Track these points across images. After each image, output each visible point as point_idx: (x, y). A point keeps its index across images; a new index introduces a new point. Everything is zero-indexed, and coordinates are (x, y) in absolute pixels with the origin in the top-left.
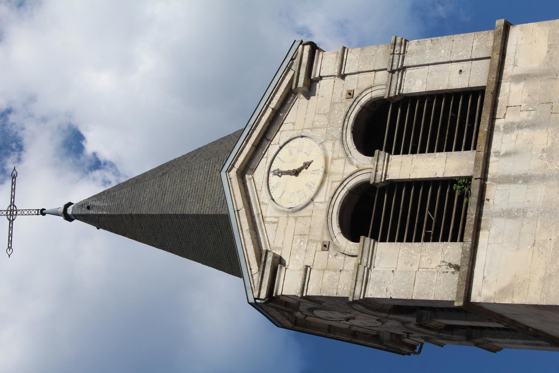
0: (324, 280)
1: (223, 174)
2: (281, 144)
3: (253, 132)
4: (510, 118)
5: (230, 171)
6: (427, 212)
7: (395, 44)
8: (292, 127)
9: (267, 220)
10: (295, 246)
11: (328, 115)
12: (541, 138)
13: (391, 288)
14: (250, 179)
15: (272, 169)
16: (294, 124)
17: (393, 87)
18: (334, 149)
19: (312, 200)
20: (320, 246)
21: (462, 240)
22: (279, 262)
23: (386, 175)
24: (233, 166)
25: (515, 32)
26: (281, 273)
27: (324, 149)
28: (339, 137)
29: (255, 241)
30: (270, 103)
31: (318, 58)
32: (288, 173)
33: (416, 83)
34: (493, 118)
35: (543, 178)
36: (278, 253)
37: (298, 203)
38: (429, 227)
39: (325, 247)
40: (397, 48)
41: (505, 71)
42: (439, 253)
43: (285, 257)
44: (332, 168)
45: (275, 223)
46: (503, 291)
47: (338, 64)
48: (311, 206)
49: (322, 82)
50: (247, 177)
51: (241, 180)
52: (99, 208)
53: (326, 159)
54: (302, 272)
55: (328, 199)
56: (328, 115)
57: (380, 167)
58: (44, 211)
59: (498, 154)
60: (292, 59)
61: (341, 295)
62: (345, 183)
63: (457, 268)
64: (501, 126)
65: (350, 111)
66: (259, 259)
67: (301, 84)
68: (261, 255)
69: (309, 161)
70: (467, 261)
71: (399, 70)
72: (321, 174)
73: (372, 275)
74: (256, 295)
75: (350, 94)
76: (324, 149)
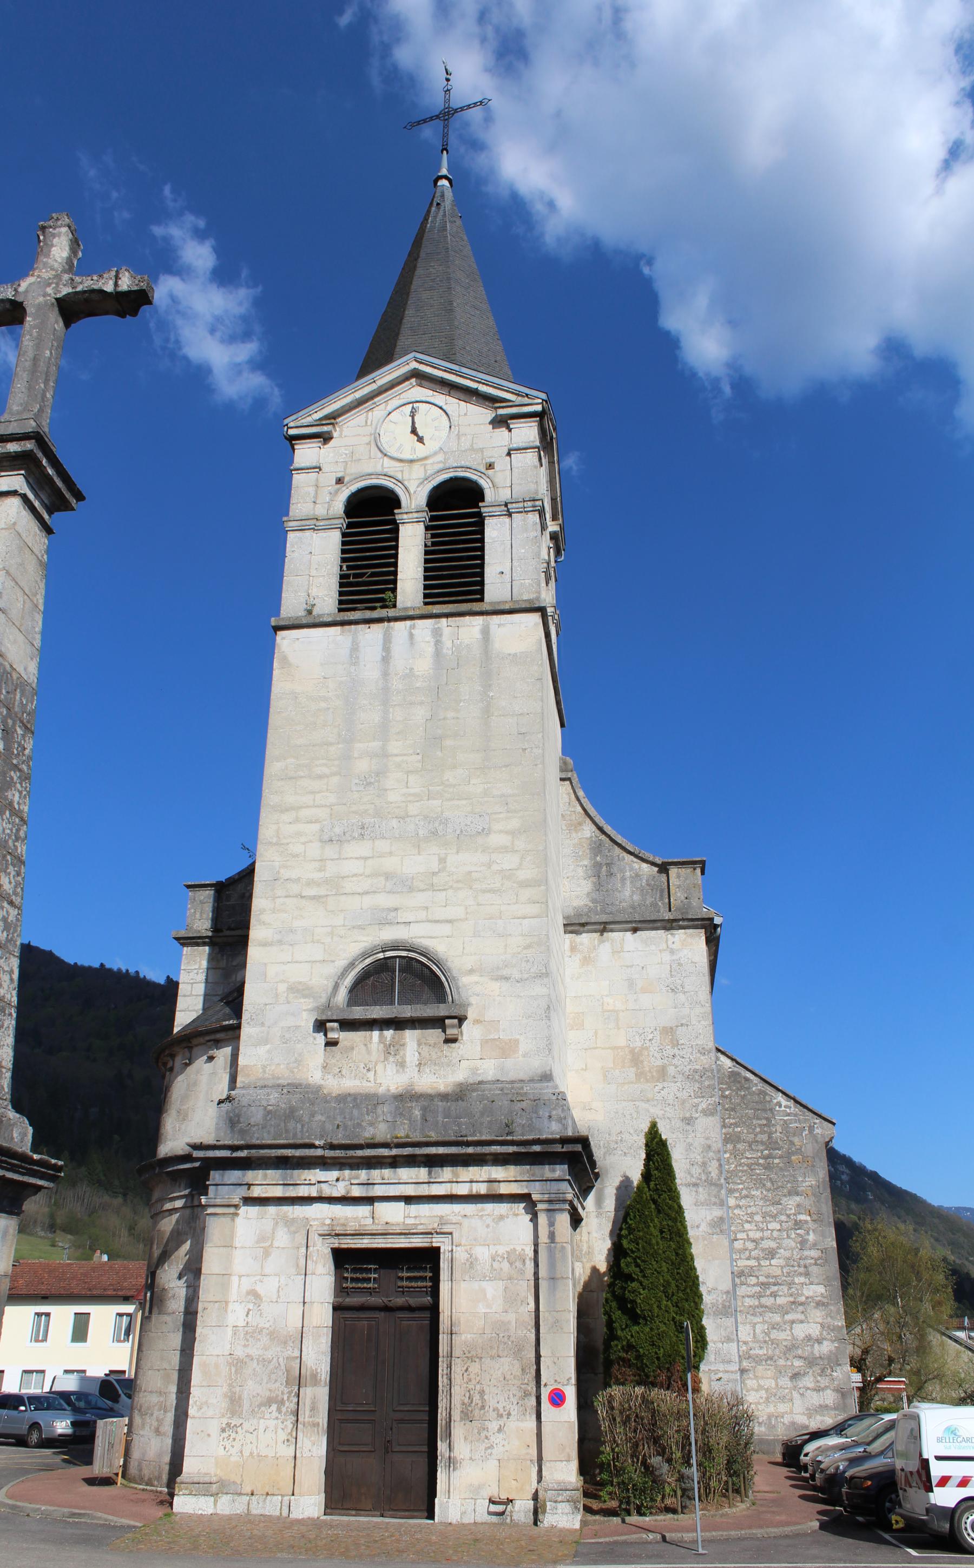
0: (306, 489)
2: (444, 407)
4: (447, 631)
6: (370, 571)
8: (462, 413)
9: (370, 413)
10: (343, 450)
11: (472, 449)
12: (424, 665)
13: (296, 554)
15: (416, 405)
16: (466, 414)
17: (491, 509)
19: (385, 455)
20: (340, 475)
21: (340, 610)
22: (326, 438)
25: (536, 618)
26: (314, 445)
27: (435, 453)
28: (447, 465)
35: (385, 674)
36: (335, 435)
37: (384, 441)
38: (355, 576)
39: (339, 481)
40: (530, 504)
41: (495, 617)
43: (332, 443)
44: (416, 466)
46: (285, 659)
47: (521, 445)
48: (380, 455)
50: (413, 381)
52: (435, 217)
53: (426, 458)
54: (314, 465)
56: (472, 449)
57: (410, 515)
59: (413, 627)
60: (527, 395)
61: (292, 507)
63: (310, 612)
66: (327, 417)
67: (501, 412)
68: (332, 418)
70: (317, 621)
71: (508, 510)
72: (411, 457)
73: (308, 533)
75: (490, 466)
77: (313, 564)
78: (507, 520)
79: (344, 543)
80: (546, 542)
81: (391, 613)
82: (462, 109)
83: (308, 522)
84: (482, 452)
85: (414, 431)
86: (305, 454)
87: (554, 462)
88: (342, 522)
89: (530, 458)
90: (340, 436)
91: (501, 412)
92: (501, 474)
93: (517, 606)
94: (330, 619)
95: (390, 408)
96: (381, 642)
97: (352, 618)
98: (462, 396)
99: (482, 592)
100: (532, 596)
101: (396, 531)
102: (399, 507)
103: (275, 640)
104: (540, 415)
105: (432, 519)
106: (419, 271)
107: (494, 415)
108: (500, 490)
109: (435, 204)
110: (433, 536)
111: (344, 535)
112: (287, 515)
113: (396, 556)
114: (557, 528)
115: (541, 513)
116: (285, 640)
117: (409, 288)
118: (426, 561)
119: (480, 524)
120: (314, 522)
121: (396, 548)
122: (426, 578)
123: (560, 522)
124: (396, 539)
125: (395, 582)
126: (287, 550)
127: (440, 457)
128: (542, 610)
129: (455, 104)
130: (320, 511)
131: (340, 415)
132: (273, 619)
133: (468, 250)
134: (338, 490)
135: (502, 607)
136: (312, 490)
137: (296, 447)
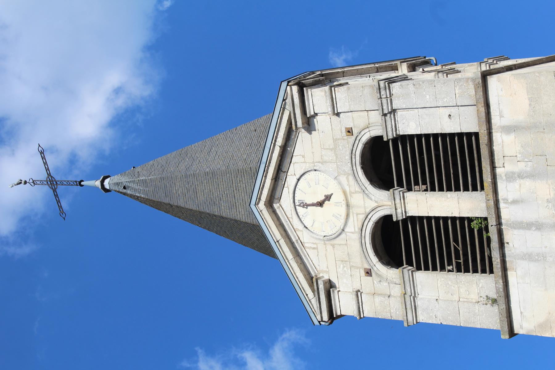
1: (252, 206)
2: (298, 177)
3: (268, 168)
4: (509, 167)
5: (258, 204)
7: (380, 89)
8: (302, 160)
9: (306, 245)
11: (334, 149)
12: (543, 189)
14: (278, 208)
15: (297, 204)
16: (303, 157)
17: (389, 129)
18: (350, 184)
19: (343, 230)
20: (363, 273)
21: (491, 272)
22: (330, 286)
23: (405, 212)
24: (260, 199)
25: (492, 81)
27: (340, 183)
28: (351, 172)
29: (302, 266)
30: (276, 141)
31: (308, 96)
32: (313, 205)
33: (409, 125)
34: (493, 167)
36: (326, 277)
37: (330, 231)
38: (457, 257)
39: (368, 273)
40: (383, 92)
41: (493, 121)
42: (475, 286)
43: (334, 280)
45: (314, 248)
46: (541, 326)
48: (343, 235)
49: (318, 118)
50: (276, 206)
51: (271, 210)
52: (135, 190)
54: (354, 297)
55: (357, 230)
57: (398, 206)
58: (82, 183)
59: (506, 201)
60: (284, 100)
61: (394, 318)
62: (369, 217)
64: (503, 175)
65: (354, 149)
66: (311, 285)
67: (300, 124)
68: (311, 280)
69: (329, 194)
70: (502, 294)
71: (390, 113)
72: (344, 206)
73: (419, 303)
74: (320, 319)
76: (340, 183)
77: (447, 297)
78: (399, 114)
79: (427, 269)
80: (418, 75)
81: (492, 222)
82: (47, 169)
83: (408, 303)
84: (336, 140)
85: (321, 204)
86: (345, 305)
87: (343, 72)
88: (407, 270)
89: (340, 93)
90: (327, 272)
91: (300, 124)
92: (357, 121)
93: (482, 100)
94: (501, 281)
95: (301, 227)
96: (522, 232)
97: (499, 260)
98: (287, 161)
99: (469, 135)
100: (471, 86)
101: (413, 219)
102: (389, 217)
103: (523, 335)
104: (301, 87)
105: (400, 185)
106: (181, 203)
107: (303, 130)
108: (371, 121)
109: (124, 191)
110: (417, 183)
111: (419, 268)
112: (402, 322)
113: (437, 219)
114: (405, 65)
115: (391, 81)
116: (522, 326)
117: (196, 211)
118: (441, 189)
119: (404, 139)
120: (407, 297)
121: (429, 219)
122: (457, 189)
123: (398, 62)
124: (421, 218)
125: (462, 219)
126: (435, 322)
127: (343, 179)
128: (485, 76)
129: (43, 176)
130: (397, 291)
131: (309, 273)
132: (502, 337)
133: (161, 160)
134: (377, 274)
135: (483, 114)
136: (378, 299)
137: (339, 314)
